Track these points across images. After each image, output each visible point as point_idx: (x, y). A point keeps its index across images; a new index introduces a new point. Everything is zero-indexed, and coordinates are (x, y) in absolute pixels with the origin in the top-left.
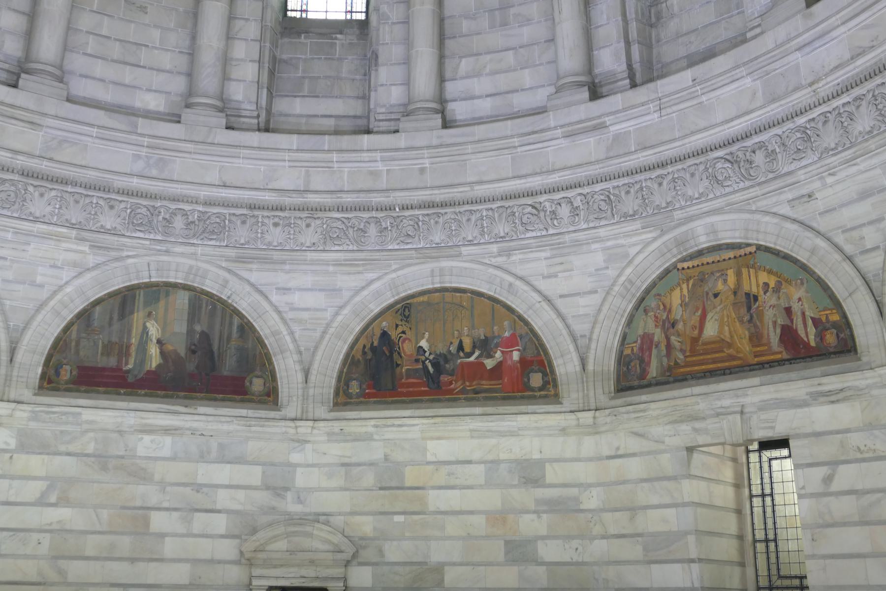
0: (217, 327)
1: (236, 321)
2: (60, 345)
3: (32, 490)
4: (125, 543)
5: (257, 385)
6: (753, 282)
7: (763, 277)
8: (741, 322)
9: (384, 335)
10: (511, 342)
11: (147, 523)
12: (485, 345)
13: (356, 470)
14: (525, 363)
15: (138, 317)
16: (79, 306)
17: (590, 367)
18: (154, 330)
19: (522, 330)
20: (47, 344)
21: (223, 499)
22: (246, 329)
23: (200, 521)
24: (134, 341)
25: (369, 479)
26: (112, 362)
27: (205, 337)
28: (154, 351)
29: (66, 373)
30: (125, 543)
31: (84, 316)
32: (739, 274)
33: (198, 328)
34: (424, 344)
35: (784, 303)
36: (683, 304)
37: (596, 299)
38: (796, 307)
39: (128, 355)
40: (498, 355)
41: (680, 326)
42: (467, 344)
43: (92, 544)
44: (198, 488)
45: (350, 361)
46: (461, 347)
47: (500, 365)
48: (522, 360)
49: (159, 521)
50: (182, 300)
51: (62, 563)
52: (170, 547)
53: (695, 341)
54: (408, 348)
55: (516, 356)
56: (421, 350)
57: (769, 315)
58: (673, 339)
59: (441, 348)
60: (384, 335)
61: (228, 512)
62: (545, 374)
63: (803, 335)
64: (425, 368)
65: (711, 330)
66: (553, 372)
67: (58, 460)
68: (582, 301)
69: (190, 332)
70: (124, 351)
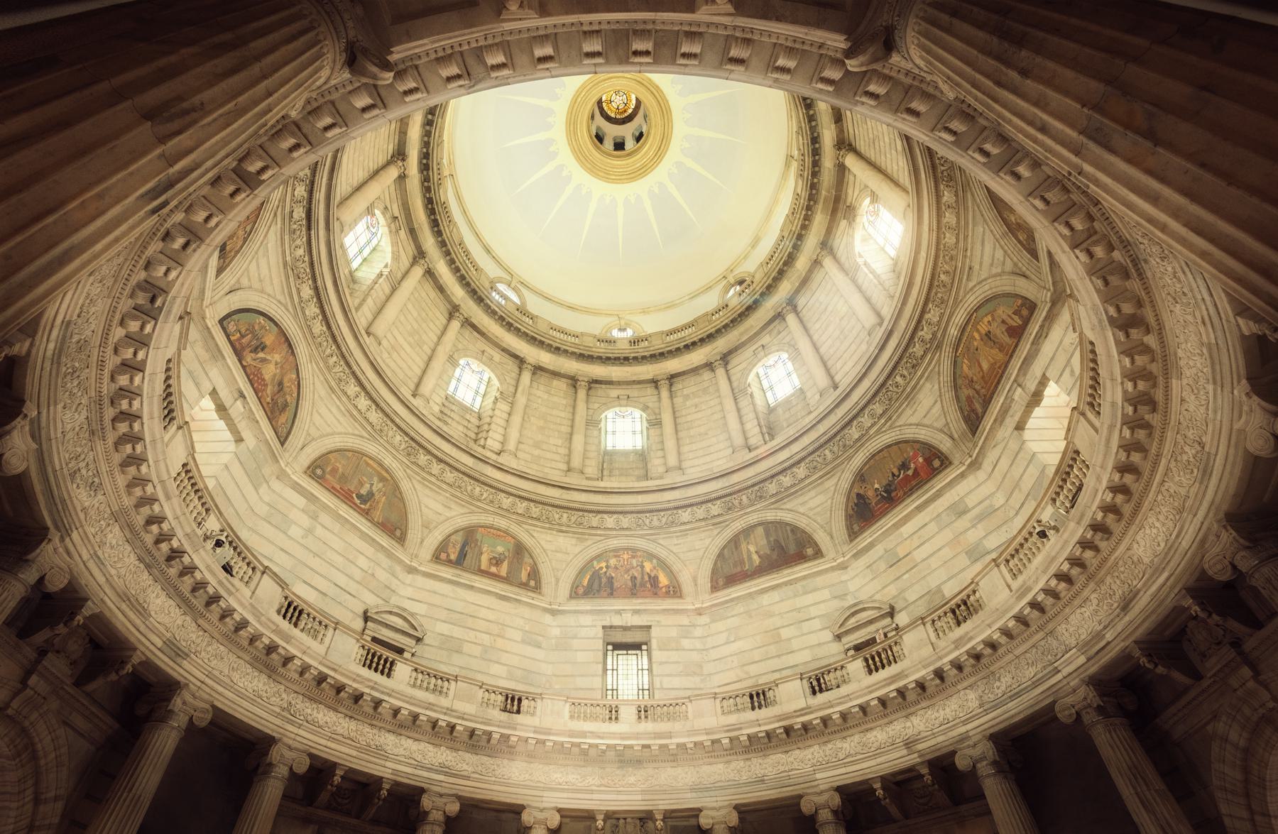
0: (781, 535)
1: (788, 528)
2: (714, 572)
3: (722, 638)
4: (773, 650)
5: (810, 551)
6: (983, 328)
7: (986, 320)
8: (992, 348)
9: (858, 495)
10: (915, 456)
11: (779, 635)
12: (904, 466)
13: (874, 567)
14: (928, 461)
15: (743, 546)
16: (717, 551)
17: (956, 436)
18: (752, 548)
19: (917, 446)
20: (709, 573)
21: (814, 611)
22: (795, 529)
23: (806, 626)
24: (745, 556)
25: (882, 565)
26: (739, 569)
27: (777, 541)
28: (755, 557)
29: (721, 582)
30: (773, 650)
31: (721, 555)
32: (978, 331)
33: (772, 539)
34: (877, 486)
35: (999, 320)
36: (970, 368)
37: (938, 405)
38: (1005, 317)
39: (744, 563)
40: (912, 466)
41: (975, 378)
42: (895, 471)
43: (757, 655)
44: (799, 610)
45: (849, 517)
46: (894, 475)
47: (916, 470)
48: (925, 460)
49: (785, 633)
50: (760, 530)
51: (746, 668)
52: (795, 644)
53: (983, 377)
54: (870, 494)
55: (921, 460)
56: (877, 490)
57: (998, 332)
58: (977, 387)
59: (885, 482)
60: (858, 495)
61: (818, 617)
62: (939, 457)
63: (1015, 324)
64: (883, 496)
65: (985, 366)
66: (942, 453)
67: (729, 621)
68: (934, 411)
69: (769, 542)
70: (742, 562)
